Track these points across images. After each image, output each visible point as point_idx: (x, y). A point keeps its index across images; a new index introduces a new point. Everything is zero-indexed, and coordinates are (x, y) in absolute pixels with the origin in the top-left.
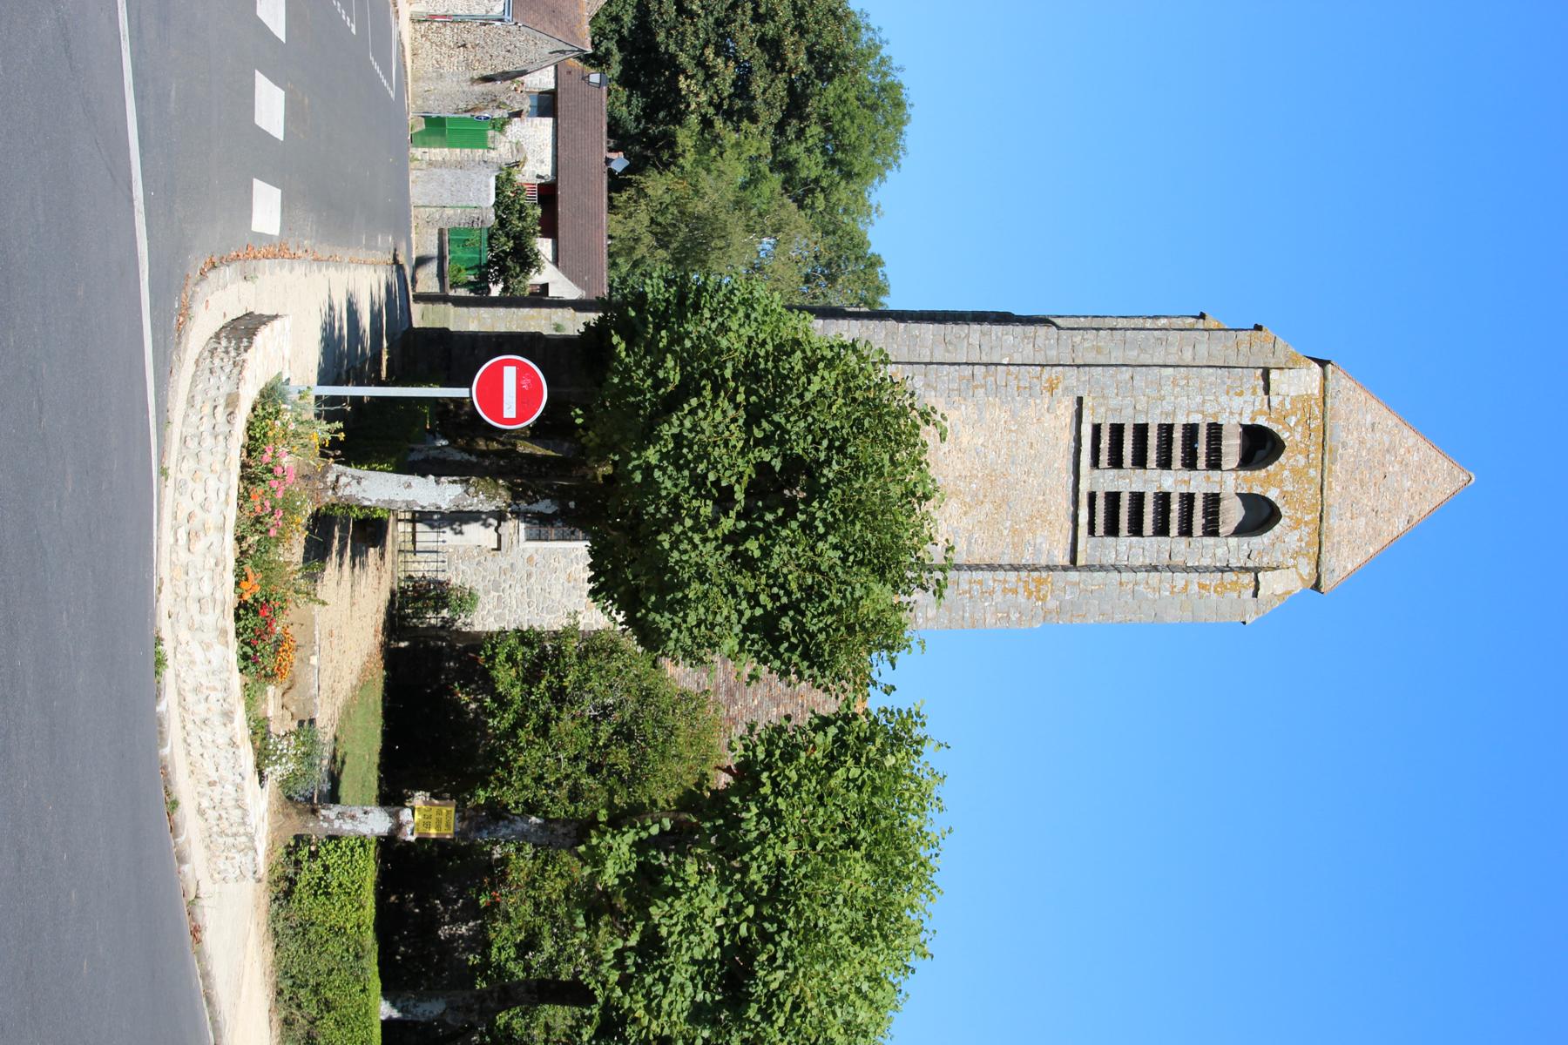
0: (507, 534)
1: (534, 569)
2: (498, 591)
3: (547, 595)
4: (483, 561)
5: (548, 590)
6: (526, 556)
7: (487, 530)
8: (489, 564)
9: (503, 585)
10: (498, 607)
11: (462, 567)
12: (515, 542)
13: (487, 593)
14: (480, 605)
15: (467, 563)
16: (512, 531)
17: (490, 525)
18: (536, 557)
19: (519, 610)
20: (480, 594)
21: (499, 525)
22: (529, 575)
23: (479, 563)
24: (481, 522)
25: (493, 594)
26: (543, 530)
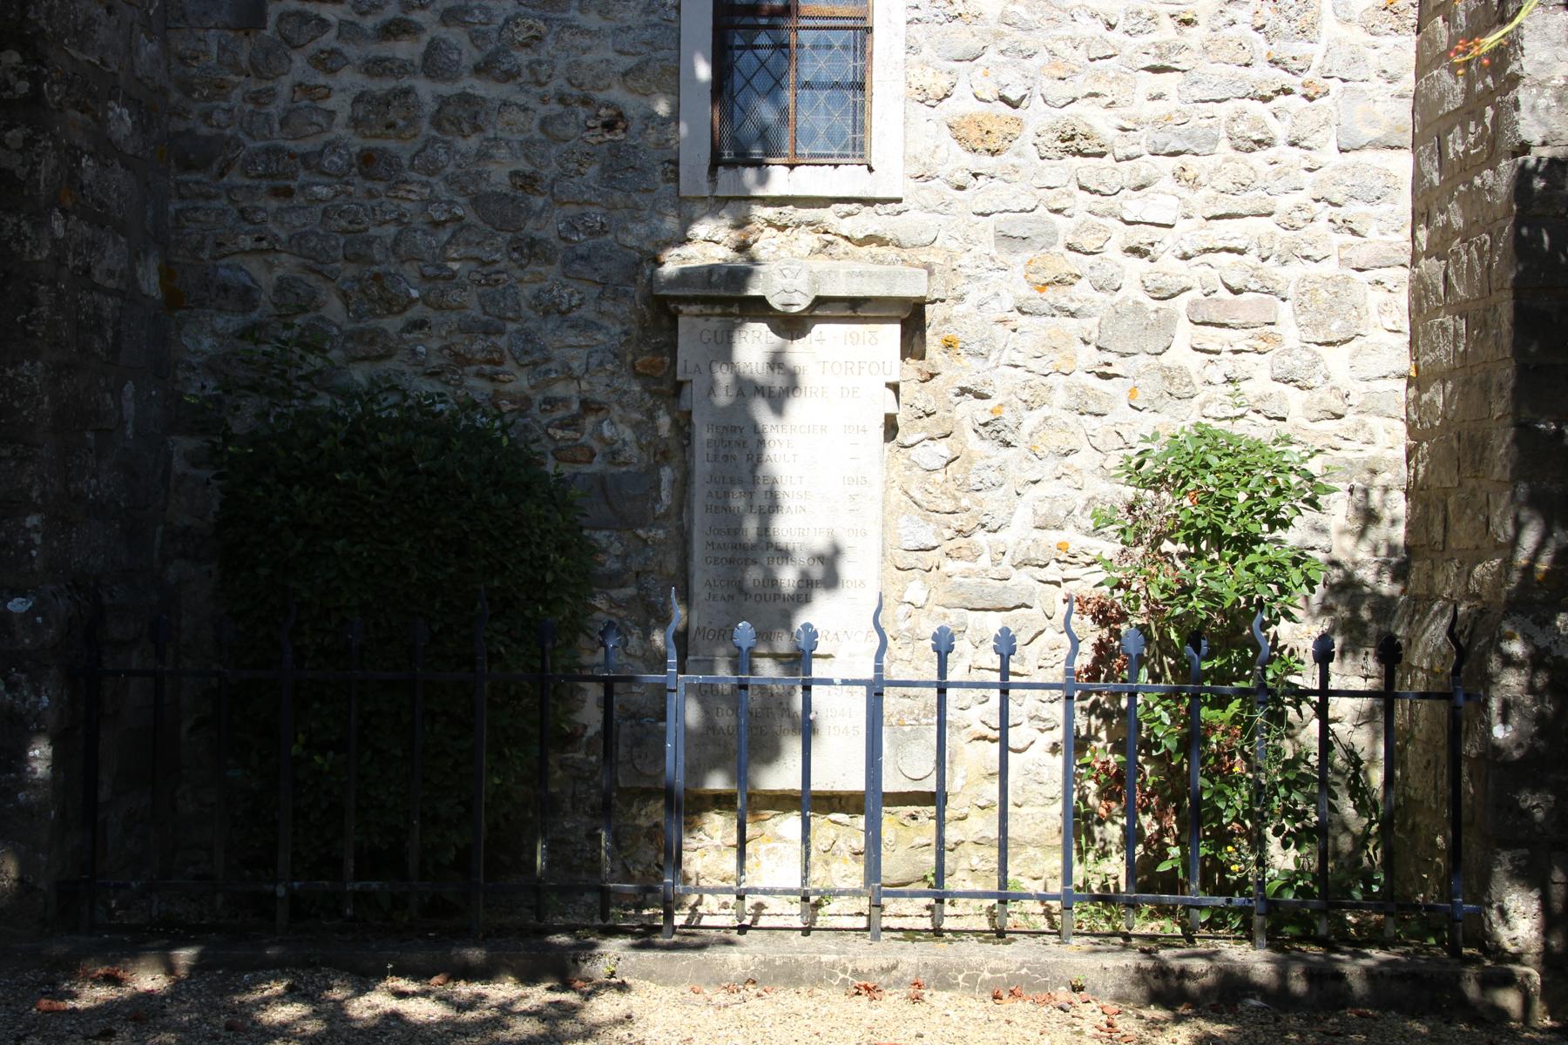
0: (821, 263)
1: (1037, 117)
2: (1165, 325)
3: (1194, 36)
4: (980, 411)
5: (1167, 32)
6: (959, 161)
7: (809, 378)
8: (1004, 384)
9: (1133, 292)
10: (1265, 334)
11: (1018, 534)
12: (866, 222)
13: (1176, 388)
14: (1256, 430)
15: (992, 502)
16: (808, 239)
17: (776, 361)
18: (962, 105)
19: (1284, 203)
20: (1178, 420)
21: (759, 309)
22: (1072, 143)
23: (996, 432)
24: (762, 413)
25: (1180, 355)
26: (813, 66)
